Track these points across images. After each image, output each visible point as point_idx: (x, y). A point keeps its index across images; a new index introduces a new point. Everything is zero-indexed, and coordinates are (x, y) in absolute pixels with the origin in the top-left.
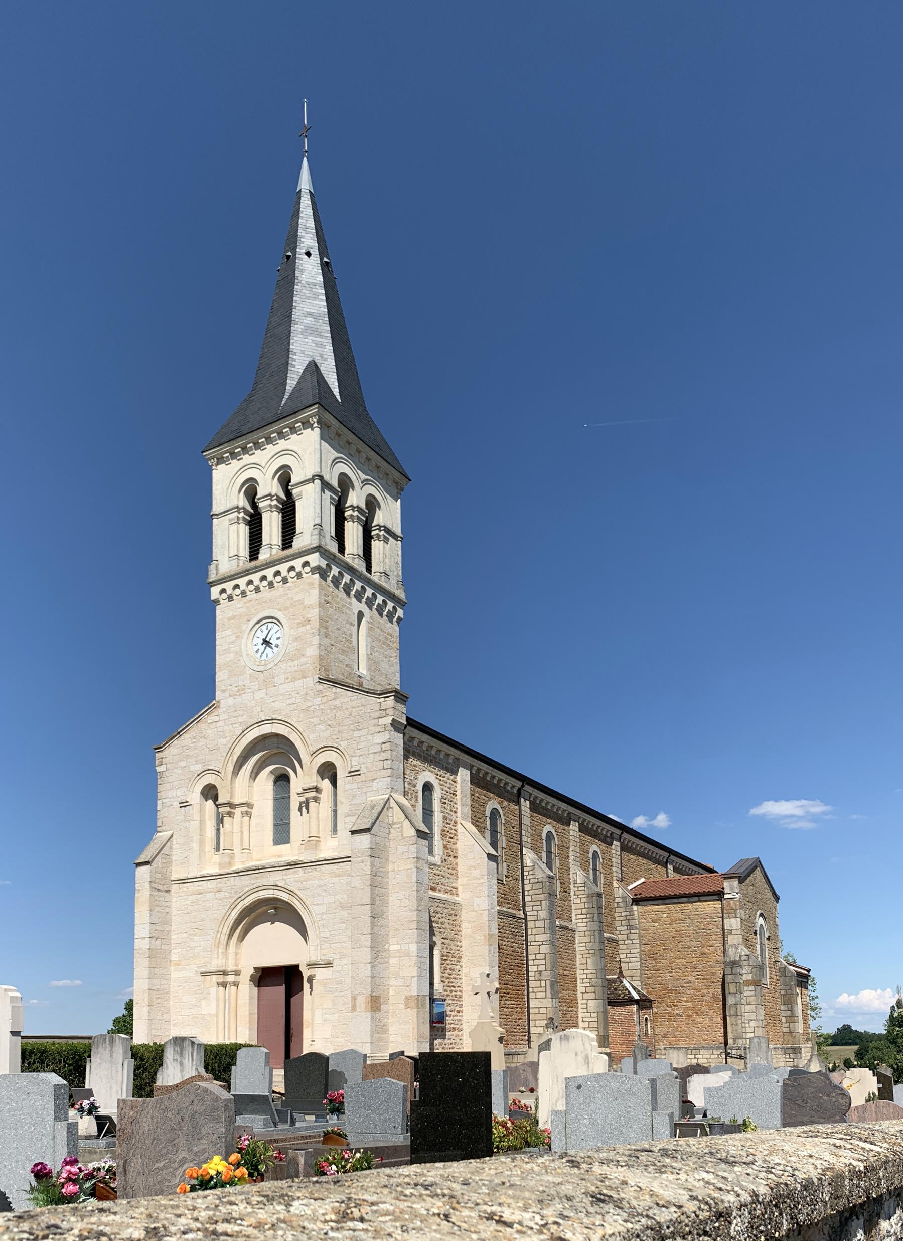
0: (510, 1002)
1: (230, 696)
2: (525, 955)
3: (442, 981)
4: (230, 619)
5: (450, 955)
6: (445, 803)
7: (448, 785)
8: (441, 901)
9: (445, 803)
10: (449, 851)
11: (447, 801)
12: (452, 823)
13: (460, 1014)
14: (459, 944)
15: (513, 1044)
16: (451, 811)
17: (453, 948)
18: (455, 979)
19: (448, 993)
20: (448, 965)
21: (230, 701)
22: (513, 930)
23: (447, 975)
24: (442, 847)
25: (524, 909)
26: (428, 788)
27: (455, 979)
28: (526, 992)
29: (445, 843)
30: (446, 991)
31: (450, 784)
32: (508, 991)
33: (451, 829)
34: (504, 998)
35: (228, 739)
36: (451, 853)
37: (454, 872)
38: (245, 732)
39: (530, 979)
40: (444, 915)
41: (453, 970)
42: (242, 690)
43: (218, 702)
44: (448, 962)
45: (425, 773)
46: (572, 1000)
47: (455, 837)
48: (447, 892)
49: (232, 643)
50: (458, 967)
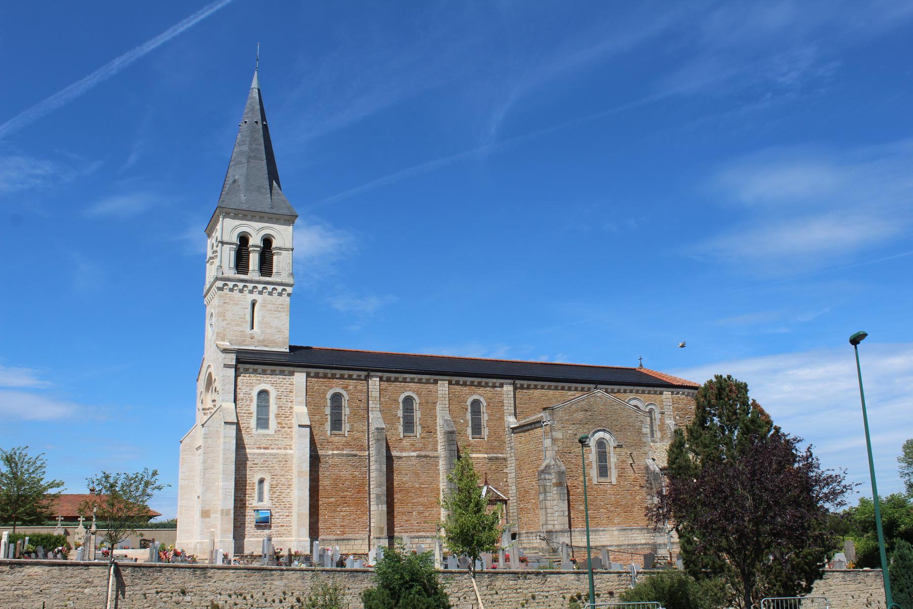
0: (348, 508)
2: (368, 478)
3: (272, 500)
5: (280, 484)
6: (279, 399)
7: (284, 388)
8: (271, 454)
9: (279, 399)
10: (284, 425)
11: (282, 397)
12: (288, 408)
13: (290, 517)
14: (289, 477)
15: (350, 533)
16: (287, 402)
17: (284, 480)
18: (284, 497)
19: (277, 506)
20: (278, 490)
22: (354, 464)
23: (276, 496)
24: (276, 423)
25: (369, 450)
26: (263, 394)
27: (284, 497)
28: (368, 502)
29: (279, 421)
30: (273, 505)
31: (286, 386)
32: (346, 502)
33: (286, 412)
34: (341, 506)
36: (286, 426)
37: (288, 436)
39: (371, 493)
40: (274, 462)
41: (282, 493)
44: (277, 488)
45: (260, 385)
46: (432, 503)
47: (291, 416)
48: (281, 449)
50: (288, 491)
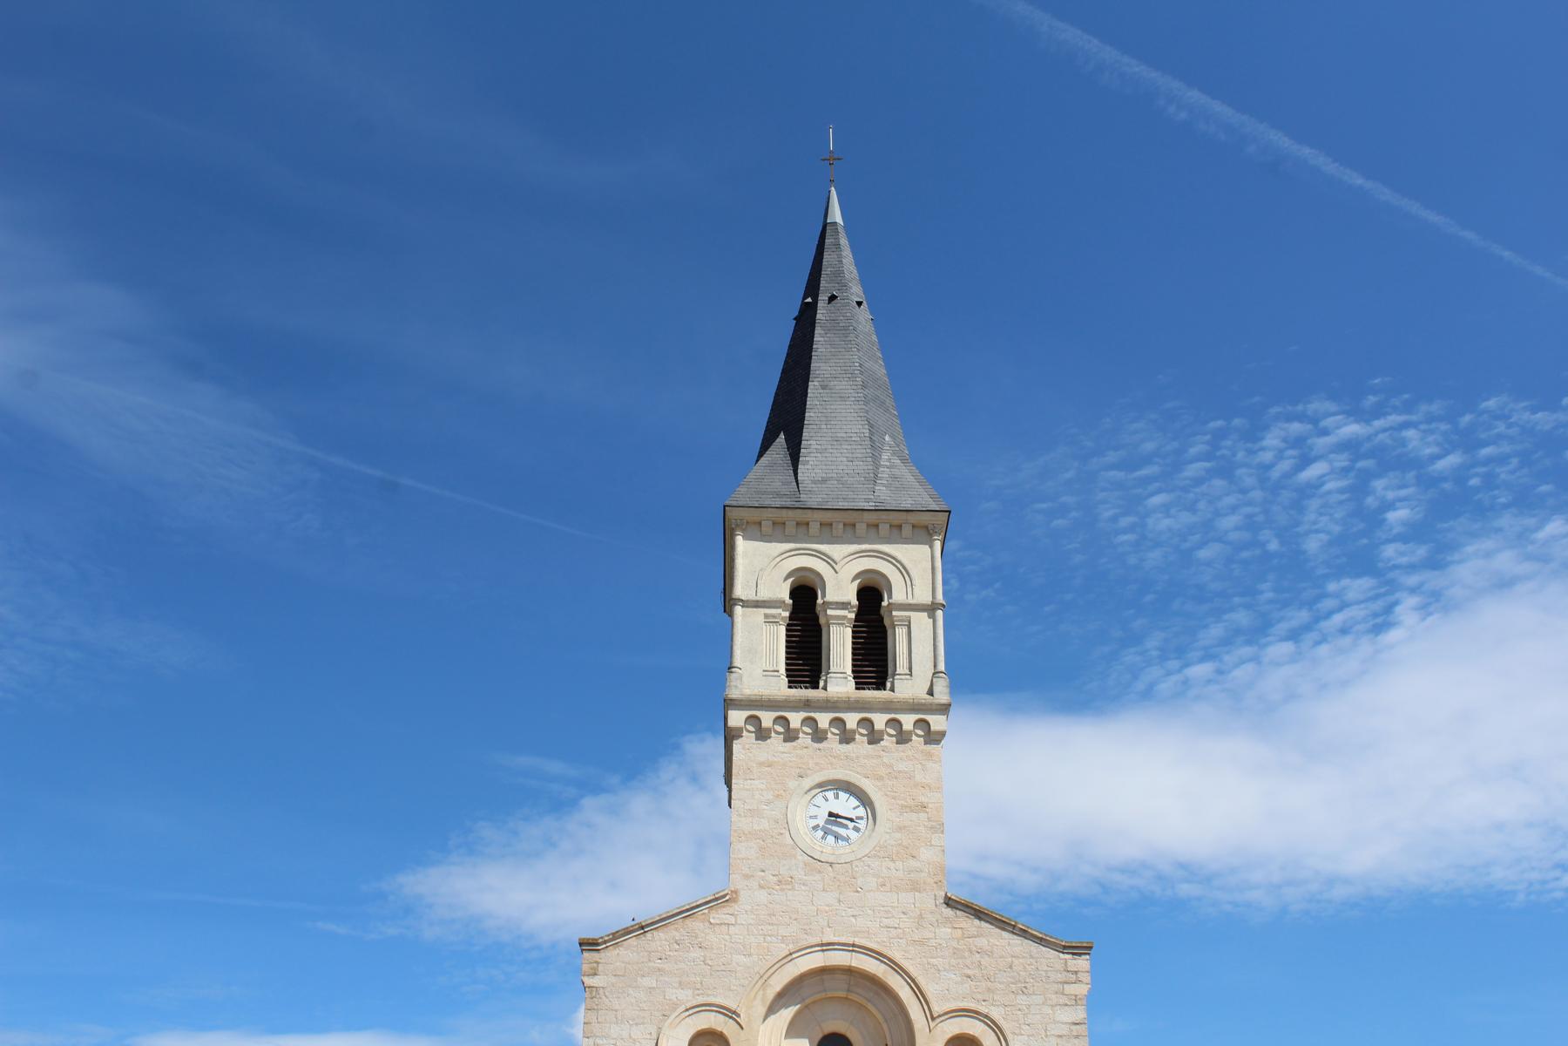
1: (761, 887)
4: (761, 764)
21: (762, 896)
35: (755, 958)
38: (794, 956)
42: (785, 883)
43: (735, 892)
49: (768, 803)
